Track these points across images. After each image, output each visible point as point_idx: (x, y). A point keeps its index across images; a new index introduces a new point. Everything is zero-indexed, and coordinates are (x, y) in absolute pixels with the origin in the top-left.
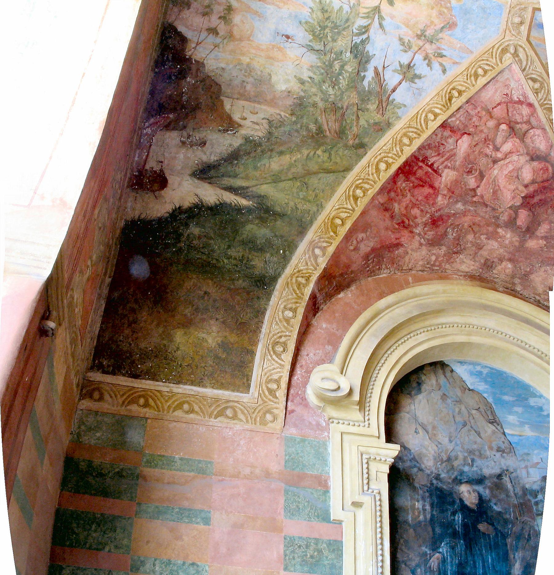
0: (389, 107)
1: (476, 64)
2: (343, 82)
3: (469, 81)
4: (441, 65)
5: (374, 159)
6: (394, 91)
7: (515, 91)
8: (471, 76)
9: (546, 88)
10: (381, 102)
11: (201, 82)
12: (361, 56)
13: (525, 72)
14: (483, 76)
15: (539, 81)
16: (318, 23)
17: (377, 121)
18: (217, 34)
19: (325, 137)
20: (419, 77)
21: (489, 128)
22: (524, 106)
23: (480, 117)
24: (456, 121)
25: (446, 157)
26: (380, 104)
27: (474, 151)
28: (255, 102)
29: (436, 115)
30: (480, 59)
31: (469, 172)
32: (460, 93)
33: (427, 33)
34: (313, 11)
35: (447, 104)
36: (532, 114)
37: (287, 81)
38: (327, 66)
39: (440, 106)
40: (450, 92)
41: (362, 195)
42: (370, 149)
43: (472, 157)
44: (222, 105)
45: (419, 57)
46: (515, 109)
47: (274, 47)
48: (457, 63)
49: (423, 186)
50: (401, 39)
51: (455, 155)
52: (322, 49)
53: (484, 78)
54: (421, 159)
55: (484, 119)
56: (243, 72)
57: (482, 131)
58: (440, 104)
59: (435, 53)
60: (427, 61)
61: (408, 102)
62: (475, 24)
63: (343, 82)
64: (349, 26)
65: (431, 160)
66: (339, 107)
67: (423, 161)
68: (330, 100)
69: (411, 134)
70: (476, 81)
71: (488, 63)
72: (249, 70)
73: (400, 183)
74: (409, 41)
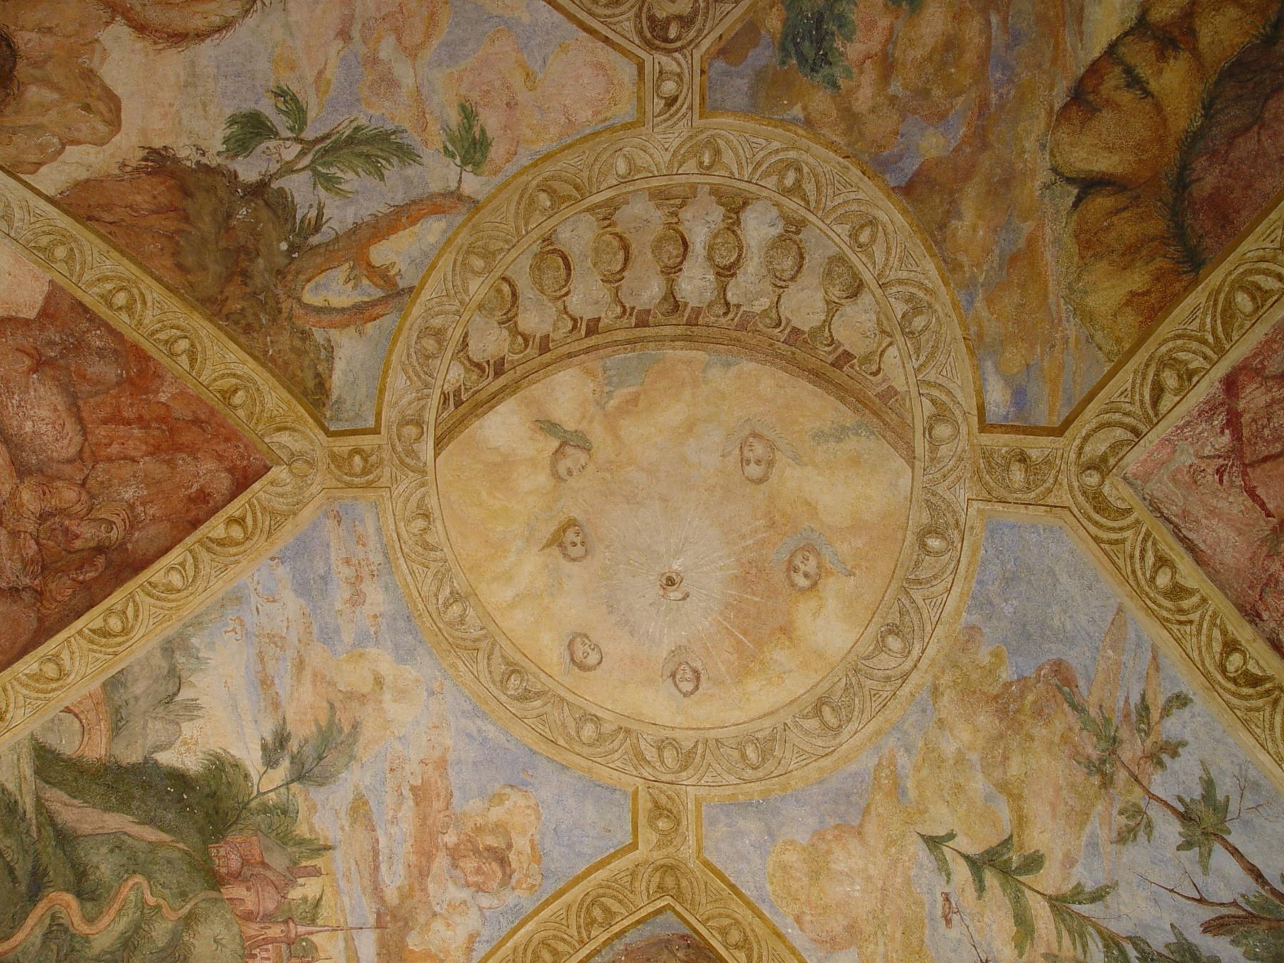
1: (1147, 594)
3: (1195, 617)
7: (1203, 447)
9: (1170, 345)
13: (1141, 426)
14: (1173, 568)
15: (1157, 375)
22: (1241, 405)
32: (1231, 646)
33: (1094, 754)
35: (1268, 692)
36: (1258, 372)
40: (1234, 681)
46: (1258, 435)
48: (1154, 658)
53: (1180, 566)
59: (1139, 730)
62: (1049, 606)
70: (1190, 592)
71: (1137, 554)
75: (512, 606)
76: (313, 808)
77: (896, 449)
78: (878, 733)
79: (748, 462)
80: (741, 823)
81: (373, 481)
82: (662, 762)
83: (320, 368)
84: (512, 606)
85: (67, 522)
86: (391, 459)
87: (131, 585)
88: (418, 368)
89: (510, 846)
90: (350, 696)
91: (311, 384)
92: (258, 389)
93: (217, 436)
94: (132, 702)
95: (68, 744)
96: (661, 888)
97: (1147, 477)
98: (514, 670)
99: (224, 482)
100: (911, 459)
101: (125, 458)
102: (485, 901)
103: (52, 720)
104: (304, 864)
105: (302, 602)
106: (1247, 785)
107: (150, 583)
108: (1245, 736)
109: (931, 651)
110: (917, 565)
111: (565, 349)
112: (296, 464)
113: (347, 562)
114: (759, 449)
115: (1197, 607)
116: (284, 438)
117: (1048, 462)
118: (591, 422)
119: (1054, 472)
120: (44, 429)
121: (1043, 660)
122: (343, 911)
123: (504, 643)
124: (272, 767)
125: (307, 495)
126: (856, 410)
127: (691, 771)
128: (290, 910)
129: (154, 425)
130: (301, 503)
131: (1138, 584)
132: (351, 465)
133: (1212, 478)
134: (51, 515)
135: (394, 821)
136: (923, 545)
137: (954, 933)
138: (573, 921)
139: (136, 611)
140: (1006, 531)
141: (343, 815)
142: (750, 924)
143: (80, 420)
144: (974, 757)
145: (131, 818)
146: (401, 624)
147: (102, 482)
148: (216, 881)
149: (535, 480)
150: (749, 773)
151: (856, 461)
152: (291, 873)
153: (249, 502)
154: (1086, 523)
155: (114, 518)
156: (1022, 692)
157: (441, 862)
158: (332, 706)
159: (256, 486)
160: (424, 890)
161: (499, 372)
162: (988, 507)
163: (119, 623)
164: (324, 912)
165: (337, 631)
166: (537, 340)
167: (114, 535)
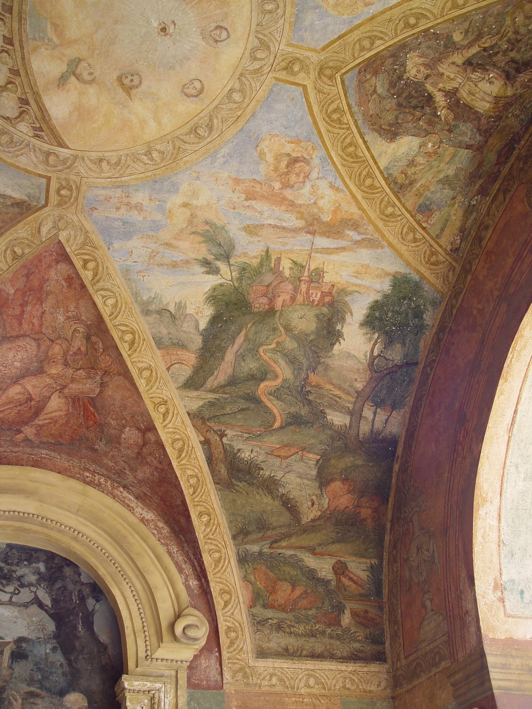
75: (160, 124)
76: (245, 254)
80: (307, 23)
81: (76, 186)
82: (262, 59)
83: (9, 203)
84: (160, 124)
85: (71, 353)
86: (66, 174)
87: (110, 325)
88: (17, 148)
89: (289, 155)
90: (190, 222)
91: (17, 210)
92: (15, 239)
93: (37, 266)
94: (170, 336)
95: (186, 372)
96: (330, 78)
98: (194, 130)
99: (63, 267)
101: (42, 317)
102: (314, 175)
103: (172, 377)
104: (273, 265)
105: (135, 237)
107: (110, 315)
111: (19, 61)
112: (60, 227)
113: (118, 209)
116: (44, 230)
118: (64, 55)
120: (20, 356)
122: (301, 250)
123: (178, 132)
124: (219, 271)
125: (77, 224)
127: (271, 45)
128: (294, 277)
129: (26, 299)
130: (82, 228)
132: (65, 196)
134: (66, 360)
135: (261, 213)
138: (336, 131)
139: (124, 325)
141: (252, 240)
142: (362, 33)
143: (18, 337)
145: (230, 348)
146: (157, 186)
147: (53, 331)
148: (271, 312)
149: (92, 96)
150: (280, 11)
152: (276, 273)
153: (76, 255)
155: (73, 328)
157: (288, 193)
158: (193, 233)
159: (68, 250)
160: (301, 206)
161: (27, 103)
163: (128, 335)
164: (300, 260)
165: (154, 222)
166: (11, 76)
167: (81, 330)
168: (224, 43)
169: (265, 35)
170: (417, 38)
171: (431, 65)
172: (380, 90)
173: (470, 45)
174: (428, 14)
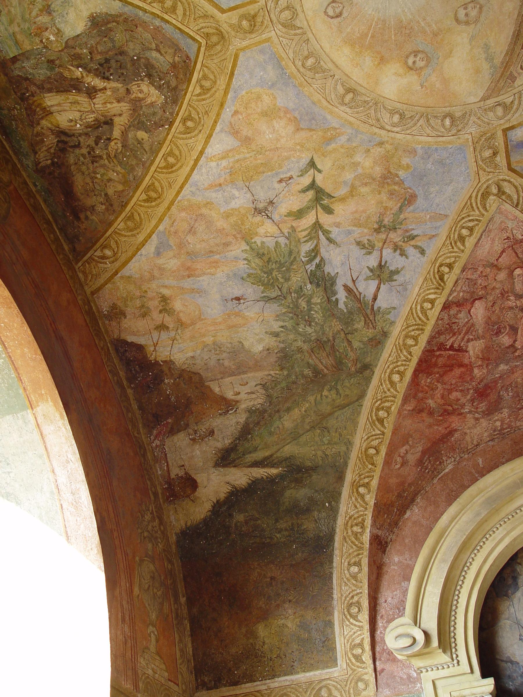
0: (378, 318)
1: (456, 226)
2: (318, 316)
3: (456, 249)
4: (416, 247)
5: (385, 375)
6: (375, 299)
7: (516, 230)
8: (455, 243)
10: (366, 316)
11: (179, 378)
12: (323, 281)
13: (520, 206)
14: (470, 235)
16: (261, 270)
17: (371, 336)
18: (168, 328)
19: (325, 375)
20: (397, 272)
21: (501, 282)
23: (486, 276)
24: (458, 294)
25: (464, 332)
26: (367, 319)
27: (493, 312)
28: (240, 374)
29: (432, 302)
30: (460, 218)
31: (498, 333)
32: (450, 266)
34: (249, 261)
35: (440, 285)
37: (261, 340)
38: (292, 308)
39: (433, 291)
40: (438, 271)
41: (386, 415)
42: (376, 366)
43: (494, 318)
44: (211, 390)
45: (387, 253)
47: (229, 316)
48: (433, 236)
49: (452, 370)
50: (358, 243)
51: (473, 325)
52: (280, 293)
53: (472, 238)
54: (435, 349)
55: (491, 275)
56: (213, 351)
57: (494, 288)
58: (433, 288)
59: (403, 238)
60: (398, 251)
61: (396, 303)
63: (318, 316)
64: (295, 258)
65: (449, 344)
66: (325, 342)
67: (439, 349)
68: (313, 338)
69: (413, 333)
70: (464, 245)
71: (471, 218)
72: (217, 347)
73: (423, 382)
74: (368, 240)
77: (487, 90)
78: (351, 123)
79: (465, 8)
80: (270, 67)
82: (281, 12)
96: (207, 36)
97: (501, 213)
100: (484, 99)
106: (404, 286)
108: (421, 280)
109: (398, 136)
110: (435, 117)
114: (474, 13)
115: (459, 249)
117: (496, 166)
119: (492, 170)
121: (414, 188)
126: (502, 63)
127: (284, 30)
131: (459, 221)
133: (505, 236)
136: (445, 117)
137: (277, 186)
140: (462, 155)
142: (218, 89)
144: (360, 171)
151: (478, 71)
154: (476, 191)
156: (397, 183)
162: (471, 144)
168: (326, 4)
169: (295, 35)
170: (171, 114)
171: (136, 105)
172: (155, 54)
173: (124, 134)
174: (184, 136)
